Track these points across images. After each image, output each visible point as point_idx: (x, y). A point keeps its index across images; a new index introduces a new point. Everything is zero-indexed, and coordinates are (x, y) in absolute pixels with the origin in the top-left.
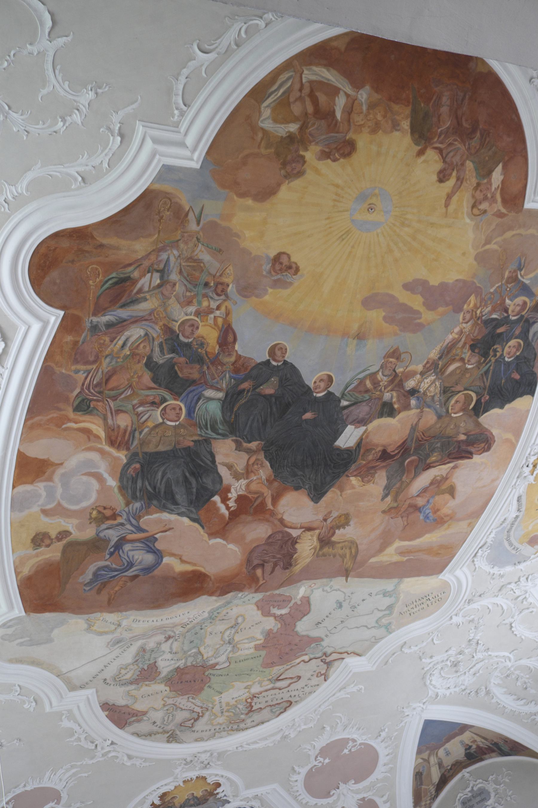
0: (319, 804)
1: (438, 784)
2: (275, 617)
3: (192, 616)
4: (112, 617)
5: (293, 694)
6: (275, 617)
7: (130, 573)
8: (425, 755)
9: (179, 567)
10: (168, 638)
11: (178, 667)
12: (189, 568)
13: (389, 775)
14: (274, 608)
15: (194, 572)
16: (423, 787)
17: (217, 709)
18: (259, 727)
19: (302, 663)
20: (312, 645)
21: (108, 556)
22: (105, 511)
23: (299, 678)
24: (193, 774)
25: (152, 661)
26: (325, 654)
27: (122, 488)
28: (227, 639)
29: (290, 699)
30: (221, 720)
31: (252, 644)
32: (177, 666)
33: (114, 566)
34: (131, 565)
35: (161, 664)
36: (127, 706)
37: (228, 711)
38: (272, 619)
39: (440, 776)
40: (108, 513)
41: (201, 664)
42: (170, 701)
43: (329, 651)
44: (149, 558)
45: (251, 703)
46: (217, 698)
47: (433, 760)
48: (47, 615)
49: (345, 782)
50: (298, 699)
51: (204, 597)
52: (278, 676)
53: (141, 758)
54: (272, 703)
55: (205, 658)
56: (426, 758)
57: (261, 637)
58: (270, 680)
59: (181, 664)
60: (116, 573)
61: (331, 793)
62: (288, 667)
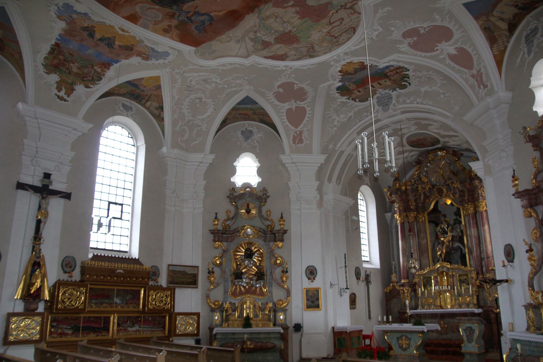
0: (433, 55)
1: (508, 29)
2: (291, 6)
3: (253, 23)
4: (223, 36)
5: (349, 24)
6: (291, 6)
7: (207, 23)
8: (484, 18)
9: (221, 14)
10: (256, 32)
11: (275, 38)
12: (225, 12)
13: (464, 34)
14: (284, 4)
15: (228, 12)
16: (495, 34)
17: (316, 42)
18: (350, 40)
19: (334, 14)
20: (329, 6)
21: (192, 24)
22: (169, 14)
23: (342, 19)
24: (343, 63)
25: (261, 41)
26: (342, 6)
27: (162, 6)
28: (281, 22)
29: (349, 27)
30: (325, 45)
31: (296, 19)
32: (274, 37)
33: (198, 25)
34: (203, 22)
35: (267, 39)
36: (274, 55)
37: (323, 41)
38: (290, 8)
39: (507, 25)
40: (171, 14)
41: (283, 34)
42: (290, 48)
43: (343, 4)
44: (205, 17)
45: (331, 35)
46: (310, 39)
47: (492, 19)
48: (203, 45)
49: (440, 42)
50: (355, 25)
51: (247, 17)
52: (329, 22)
53: (310, 65)
54: (344, 31)
55: (282, 31)
56: (486, 19)
57: (295, 15)
58: (327, 25)
59: (274, 36)
60: (203, 26)
61: (435, 49)
62: (329, 18)
